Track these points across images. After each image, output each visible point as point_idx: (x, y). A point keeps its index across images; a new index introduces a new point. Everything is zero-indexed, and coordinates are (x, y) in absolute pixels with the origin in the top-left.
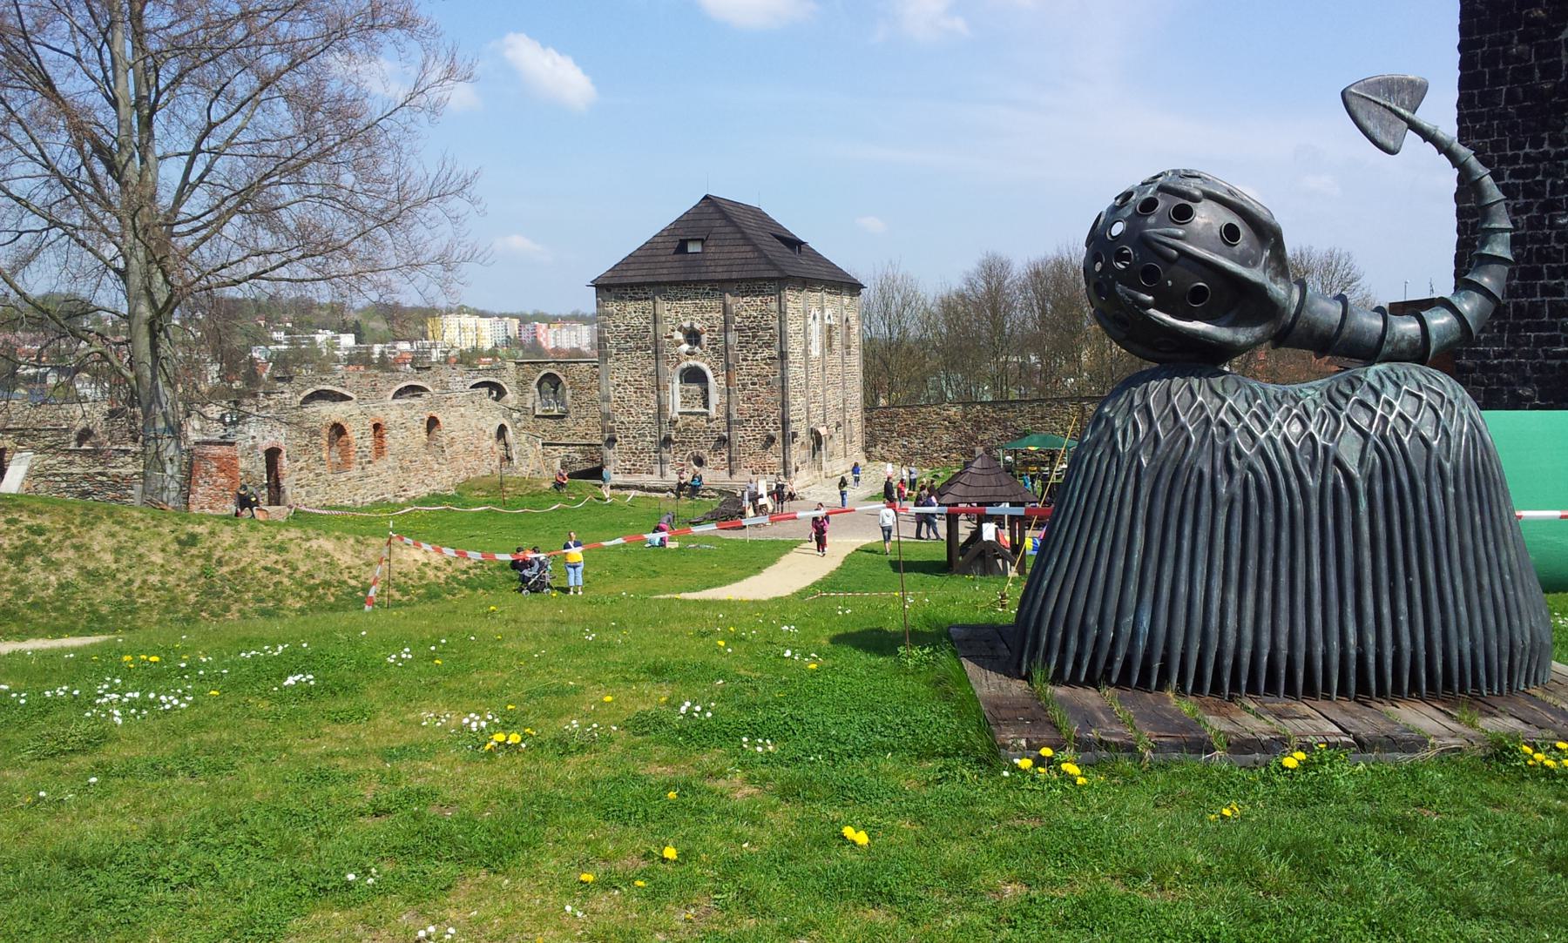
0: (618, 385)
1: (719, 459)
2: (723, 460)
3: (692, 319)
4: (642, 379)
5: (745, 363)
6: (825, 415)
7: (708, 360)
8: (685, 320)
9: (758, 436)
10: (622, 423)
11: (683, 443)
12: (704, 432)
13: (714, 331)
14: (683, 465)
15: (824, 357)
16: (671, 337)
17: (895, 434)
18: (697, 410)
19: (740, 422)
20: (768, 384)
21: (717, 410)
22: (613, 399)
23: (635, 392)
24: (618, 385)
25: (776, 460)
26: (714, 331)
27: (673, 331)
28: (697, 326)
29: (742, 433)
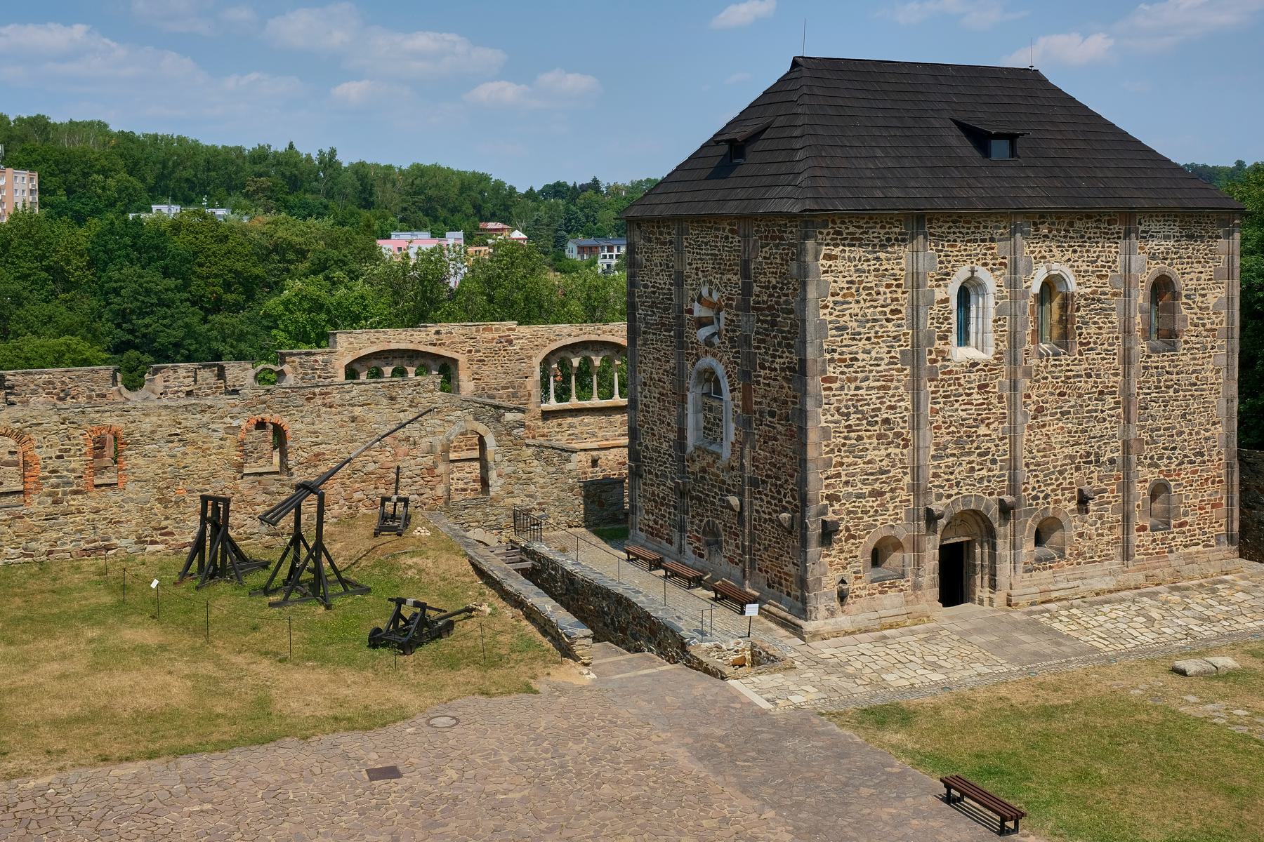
6: (1013, 479)
15: (1014, 361)
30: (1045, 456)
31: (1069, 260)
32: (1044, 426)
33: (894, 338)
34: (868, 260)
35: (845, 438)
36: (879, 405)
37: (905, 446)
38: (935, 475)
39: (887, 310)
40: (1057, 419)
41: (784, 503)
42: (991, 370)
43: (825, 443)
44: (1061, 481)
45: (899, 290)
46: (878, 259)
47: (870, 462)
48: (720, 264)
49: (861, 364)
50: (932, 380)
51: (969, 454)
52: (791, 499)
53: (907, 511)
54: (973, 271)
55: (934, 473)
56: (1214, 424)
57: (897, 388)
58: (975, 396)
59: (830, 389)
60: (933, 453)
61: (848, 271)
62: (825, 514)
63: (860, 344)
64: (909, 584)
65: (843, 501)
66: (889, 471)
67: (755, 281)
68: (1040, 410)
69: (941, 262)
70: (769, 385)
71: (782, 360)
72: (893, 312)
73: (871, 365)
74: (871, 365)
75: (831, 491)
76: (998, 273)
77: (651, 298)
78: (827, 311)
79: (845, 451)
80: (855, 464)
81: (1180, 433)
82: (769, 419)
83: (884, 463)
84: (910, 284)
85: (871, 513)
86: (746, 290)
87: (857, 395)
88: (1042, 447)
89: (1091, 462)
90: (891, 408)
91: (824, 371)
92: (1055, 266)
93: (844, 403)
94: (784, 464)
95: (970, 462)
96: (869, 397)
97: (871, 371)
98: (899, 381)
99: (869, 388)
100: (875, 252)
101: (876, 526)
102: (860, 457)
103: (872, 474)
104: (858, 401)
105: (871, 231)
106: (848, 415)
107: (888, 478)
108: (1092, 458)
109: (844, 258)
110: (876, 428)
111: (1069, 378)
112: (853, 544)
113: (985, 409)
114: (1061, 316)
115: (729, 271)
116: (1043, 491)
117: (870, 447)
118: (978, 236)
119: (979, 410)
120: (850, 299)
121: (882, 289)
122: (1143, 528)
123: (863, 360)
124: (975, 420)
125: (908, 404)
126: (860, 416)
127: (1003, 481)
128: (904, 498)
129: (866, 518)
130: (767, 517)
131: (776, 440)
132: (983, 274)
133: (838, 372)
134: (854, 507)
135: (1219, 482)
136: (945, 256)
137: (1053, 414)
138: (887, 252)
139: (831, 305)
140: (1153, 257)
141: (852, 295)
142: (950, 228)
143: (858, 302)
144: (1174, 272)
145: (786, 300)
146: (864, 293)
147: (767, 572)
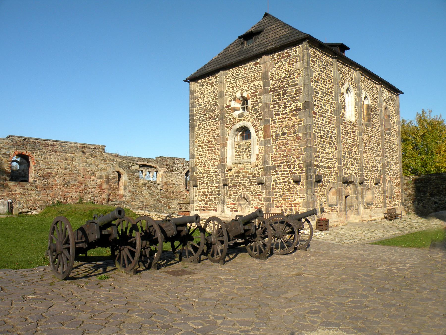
0: (199, 146)
1: (258, 200)
2: (261, 200)
3: (242, 90)
4: (213, 140)
5: (277, 117)
7: (252, 119)
8: (238, 91)
9: (287, 179)
10: (201, 173)
11: (235, 186)
12: (249, 177)
13: (256, 96)
14: (234, 204)
16: (229, 106)
17: (428, 194)
18: (246, 160)
19: (274, 168)
20: (295, 132)
21: (258, 159)
22: (196, 157)
23: (208, 150)
24: (199, 146)
25: (300, 201)
26: (256, 96)
27: (230, 101)
28: (245, 95)
29: (274, 178)
30: (367, 164)
31: (369, 92)
32: (366, 153)
33: (332, 103)
34: (323, 68)
35: (320, 141)
36: (328, 130)
37: (336, 150)
38: (344, 165)
39: (329, 90)
40: (369, 151)
41: (293, 171)
42: (355, 126)
43: (315, 141)
44: (371, 175)
45: (332, 84)
46: (325, 68)
47: (327, 153)
48: (248, 80)
49: (324, 110)
50: (342, 124)
51: (351, 158)
52: (298, 169)
53: (337, 177)
54: (349, 86)
55: (344, 163)
56: (398, 163)
57: (333, 124)
58: (352, 135)
59: (315, 117)
60: (343, 155)
61: (318, 69)
62: (316, 173)
63: (323, 101)
64: (338, 209)
65: (320, 169)
66: (331, 159)
67: (272, 79)
68: (366, 146)
69: (342, 78)
70: (282, 122)
71: (290, 108)
72: (331, 92)
73: (326, 112)
74: (326, 112)
75: (317, 163)
76: (354, 89)
77: (203, 109)
78: (313, 83)
79: (321, 146)
80: (323, 153)
81: (392, 165)
82: (282, 137)
83: (331, 155)
84: (334, 83)
85: (328, 176)
86: (266, 84)
87: (322, 123)
88: (367, 160)
89: (376, 170)
90: (332, 132)
91: (313, 109)
92: (367, 93)
93: (319, 125)
94: (293, 154)
95: (352, 161)
96: (326, 125)
97: (326, 114)
98: (333, 122)
99: (326, 122)
100: (325, 66)
101: (329, 182)
102: (325, 150)
103: (327, 159)
104: (323, 126)
105: (323, 56)
106: (320, 130)
107: (332, 162)
108: (377, 168)
109: (316, 63)
110: (328, 139)
111: (371, 136)
112: (324, 188)
113: (354, 141)
114: (367, 113)
115: (253, 81)
116: (367, 178)
117: (327, 147)
118: (349, 73)
119: (353, 141)
120: (319, 82)
121: (327, 82)
122: (387, 197)
123: (324, 109)
124: (352, 144)
125: (335, 131)
126: (324, 132)
127: (359, 171)
128: (336, 172)
129: (326, 178)
130: (282, 181)
131: (287, 144)
132: (351, 87)
133: (317, 111)
134: (323, 172)
135: (400, 184)
136: (343, 76)
137: (369, 149)
138: (328, 67)
139: (314, 82)
140: (384, 100)
141: (320, 80)
142: (343, 66)
143: (321, 84)
144: (389, 107)
145: (293, 81)
146: (323, 81)
147: (281, 207)
